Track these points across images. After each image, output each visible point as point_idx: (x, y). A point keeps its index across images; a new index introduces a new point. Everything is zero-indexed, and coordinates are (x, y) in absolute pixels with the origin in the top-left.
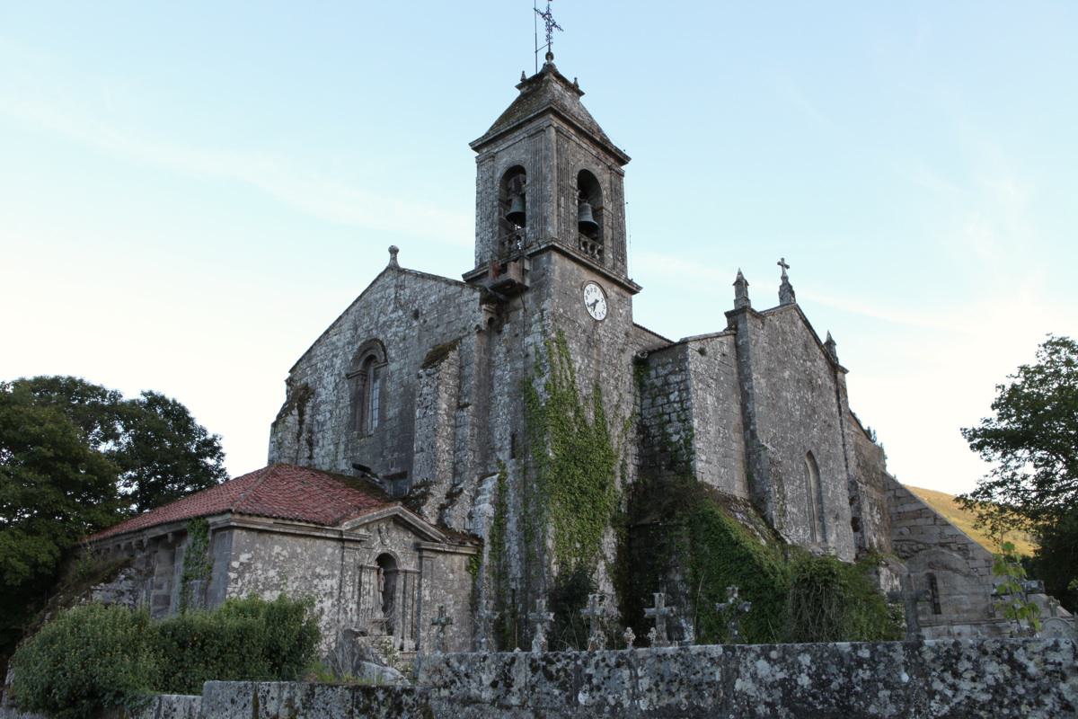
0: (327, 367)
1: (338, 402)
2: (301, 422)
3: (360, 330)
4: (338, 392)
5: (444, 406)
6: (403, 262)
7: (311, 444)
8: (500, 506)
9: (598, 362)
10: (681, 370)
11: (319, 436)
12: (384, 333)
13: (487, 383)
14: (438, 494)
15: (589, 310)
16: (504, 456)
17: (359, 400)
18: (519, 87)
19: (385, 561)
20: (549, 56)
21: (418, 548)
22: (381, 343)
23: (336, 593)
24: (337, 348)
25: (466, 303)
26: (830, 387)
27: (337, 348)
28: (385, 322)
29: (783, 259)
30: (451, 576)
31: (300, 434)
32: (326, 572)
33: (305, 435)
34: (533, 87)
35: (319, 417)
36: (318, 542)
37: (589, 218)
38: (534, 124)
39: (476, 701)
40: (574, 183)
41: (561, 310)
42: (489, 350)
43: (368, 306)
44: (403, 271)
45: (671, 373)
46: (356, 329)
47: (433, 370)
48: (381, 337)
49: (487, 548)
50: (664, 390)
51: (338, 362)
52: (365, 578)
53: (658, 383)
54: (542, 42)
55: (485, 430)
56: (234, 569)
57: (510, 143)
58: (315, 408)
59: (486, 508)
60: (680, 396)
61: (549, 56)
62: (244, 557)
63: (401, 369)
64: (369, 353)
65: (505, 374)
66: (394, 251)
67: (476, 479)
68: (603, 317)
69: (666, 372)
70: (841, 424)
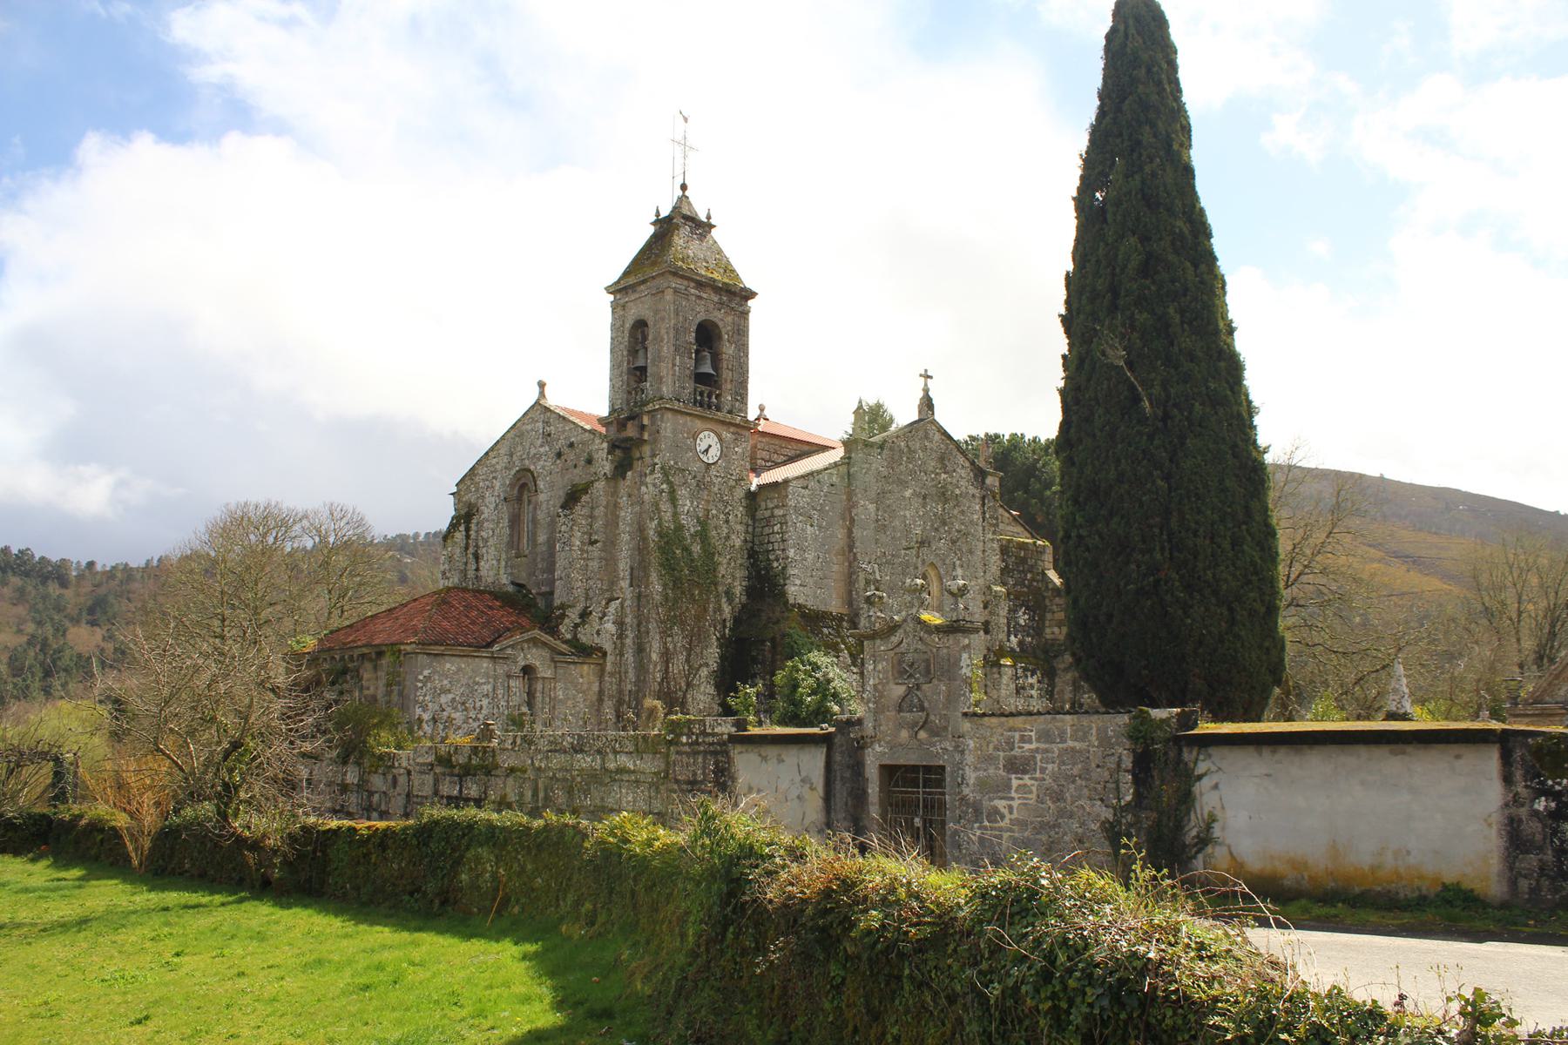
1: (498, 522)
2: (468, 537)
3: (515, 458)
5: (578, 543)
6: (553, 400)
7: (477, 557)
8: (620, 624)
9: (708, 501)
10: (783, 506)
11: (484, 550)
12: (534, 464)
13: (613, 522)
14: (573, 615)
15: (701, 456)
16: (625, 584)
17: (515, 521)
18: (654, 223)
19: (528, 671)
20: (684, 187)
21: (553, 660)
22: (532, 473)
23: (491, 695)
24: (495, 471)
25: (598, 450)
26: (973, 496)
27: (495, 471)
28: (535, 454)
29: (926, 371)
30: (581, 680)
31: (467, 548)
32: (483, 681)
33: (471, 550)
34: (665, 228)
35: (483, 534)
36: (477, 659)
37: (707, 368)
38: (656, 282)
39: (507, 749)
40: (692, 337)
41: (672, 463)
43: (521, 435)
44: (547, 409)
45: (777, 507)
46: (511, 455)
47: (568, 512)
48: (532, 468)
49: (610, 659)
51: (497, 484)
52: (512, 683)
54: (679, 171)
55: (610, 562)
56: (420, 681)
57: (637, 296)
59: (610, 627)
60: (781, 528)
61: (684, 187)
62: (426, 673)
63: (548, 501)
64: (521, 482)
65: (627, 514)
66: (542, 385)
67: (604, 603)
68: (715, 460)
70: (984, 530)
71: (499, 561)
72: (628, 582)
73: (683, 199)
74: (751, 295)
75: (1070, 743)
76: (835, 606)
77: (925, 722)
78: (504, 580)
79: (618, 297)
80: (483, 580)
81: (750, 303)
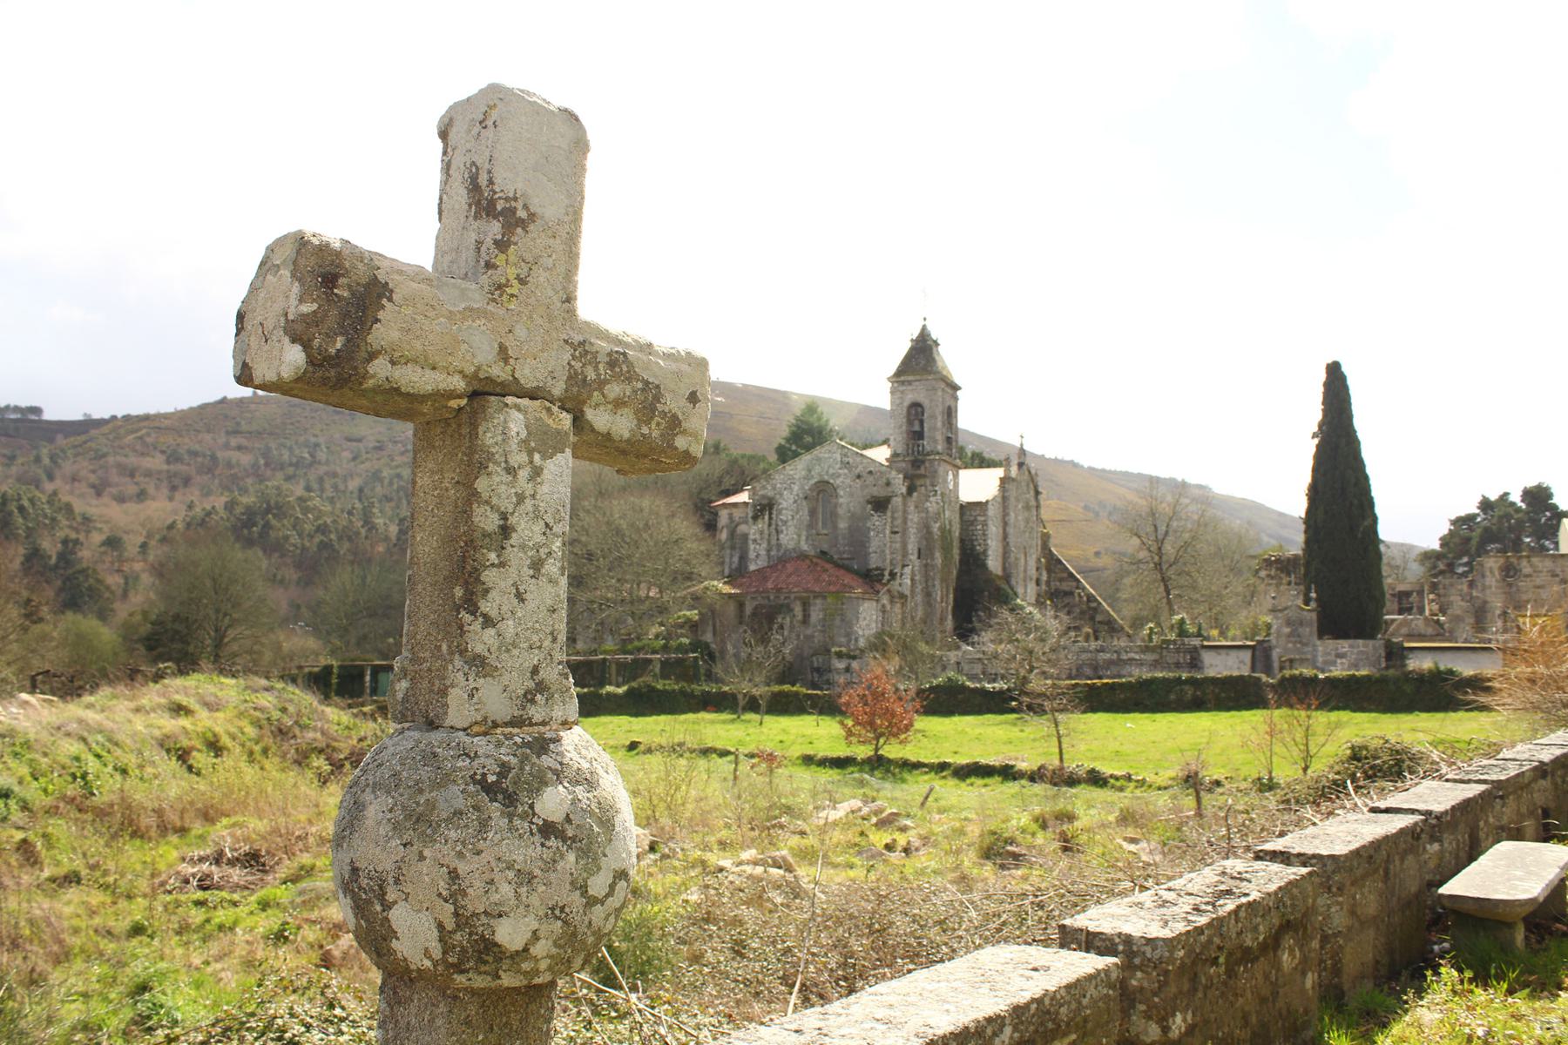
2: (770, 518)
7: (778, 532)
16: (914, 557)
42: (905, 504)
46: (810, 471)
50: (972, 523)
51: (796, 488)
58: (780, 512)
65: (914, 518)
71: (799, 536)
73: (924, 328)
74: (959, 388)
76: (1000, 572)
78: (805, 547)
81: (959, 393)
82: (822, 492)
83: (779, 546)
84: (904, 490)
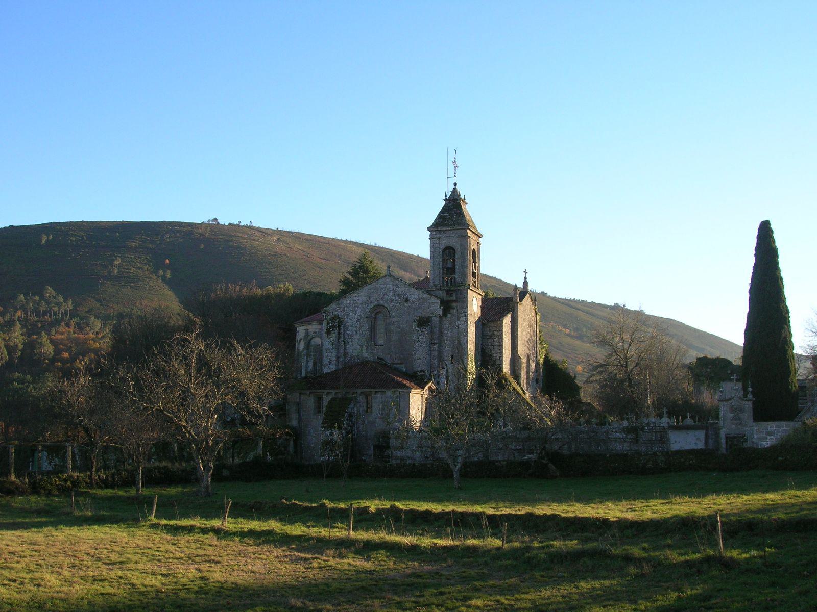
0: (351, 310)
2: (339, 333)
3: (372, 299)
4: (360, 324)
12: (387, 304)
20: (455, 184)
31: (339, 338)
45: (495, 331)
48: (386, 305)
53: (490, 333)
54: (452, 174)
58: (346, 328)
61: (455, 184)
69: (493, 330)
71: (361, 347)
72: (450, 362)
73: (455, 190)
75: (785, 428)
77: (741, 423)
78: (366, 355)
79: (434, 233)
80: (350, 354)
82: (378, 311)
83: (346, 354)
84: (441, 313)
